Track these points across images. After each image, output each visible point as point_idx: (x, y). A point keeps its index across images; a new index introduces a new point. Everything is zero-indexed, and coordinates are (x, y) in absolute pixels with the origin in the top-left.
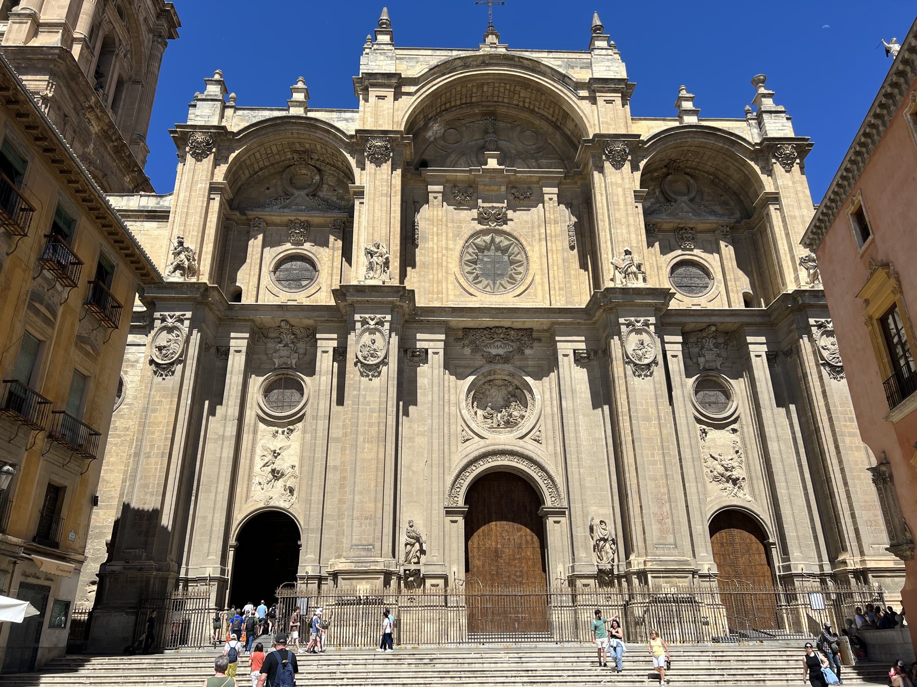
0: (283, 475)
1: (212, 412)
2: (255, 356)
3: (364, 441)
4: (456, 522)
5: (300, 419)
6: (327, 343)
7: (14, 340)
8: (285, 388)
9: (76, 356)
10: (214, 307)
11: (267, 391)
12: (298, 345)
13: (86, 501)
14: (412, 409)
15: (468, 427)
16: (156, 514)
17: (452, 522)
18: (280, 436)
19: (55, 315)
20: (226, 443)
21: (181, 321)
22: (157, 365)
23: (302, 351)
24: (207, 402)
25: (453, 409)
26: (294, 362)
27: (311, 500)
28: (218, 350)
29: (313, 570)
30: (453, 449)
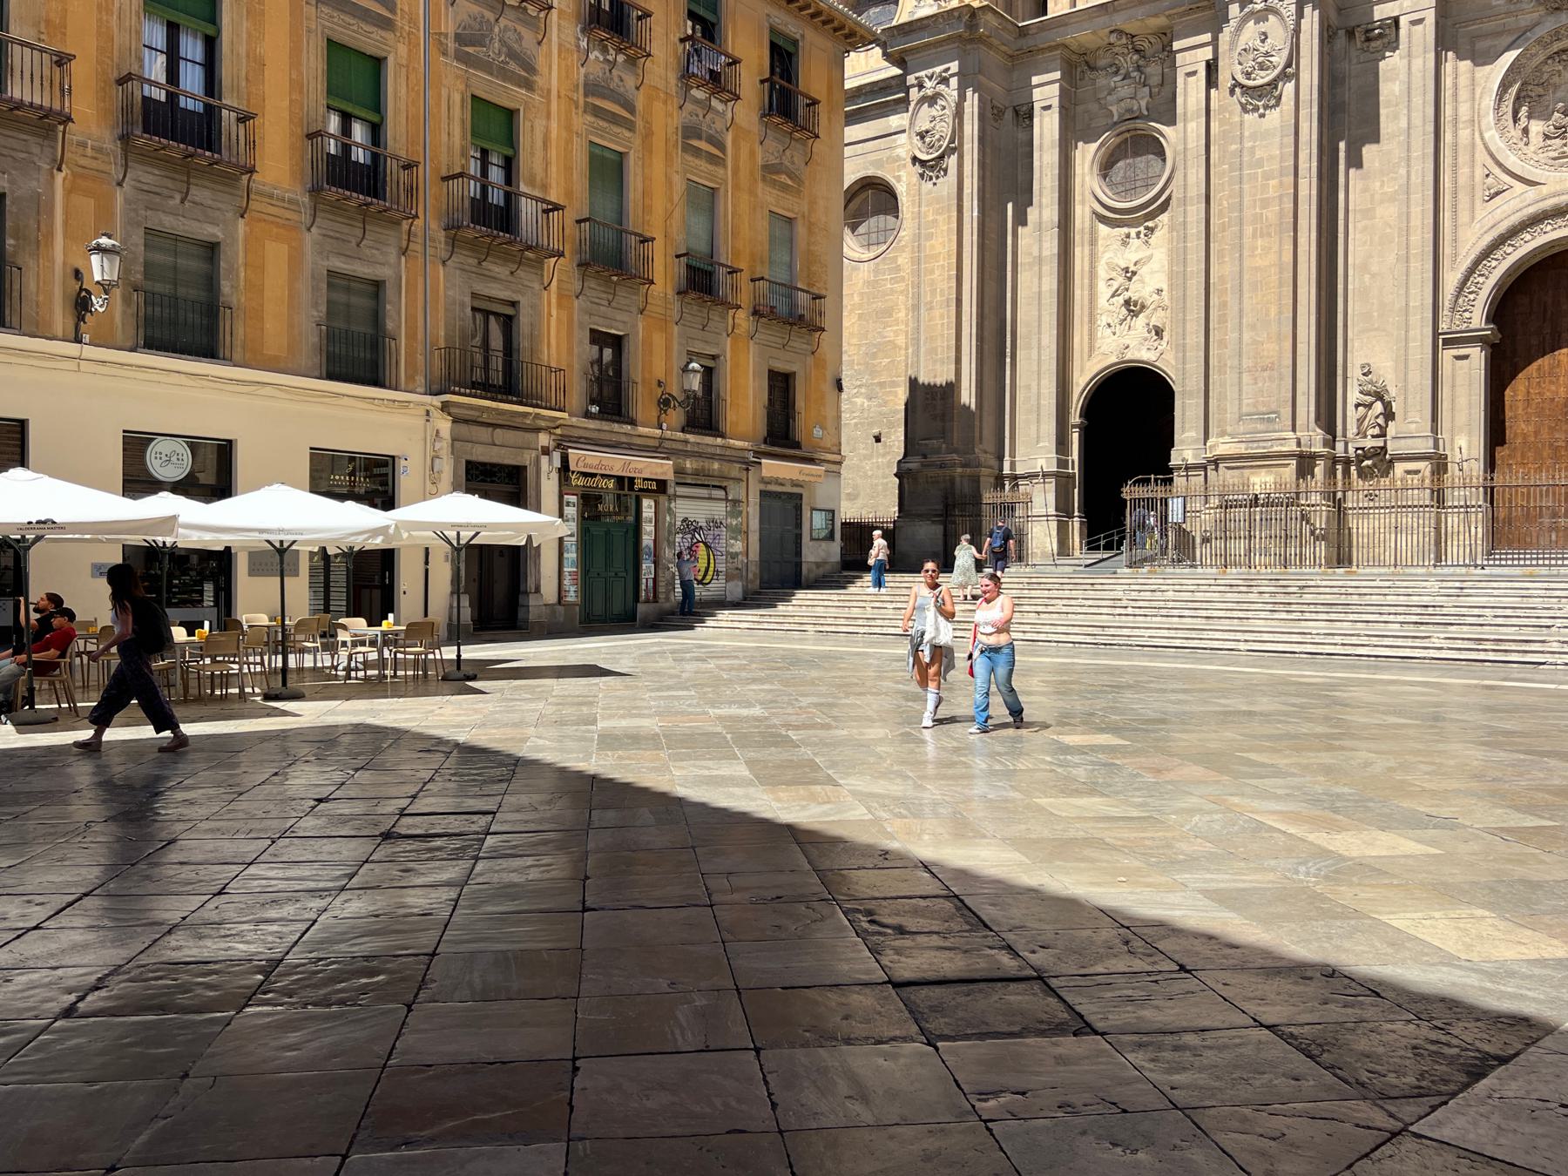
0: (1143, 307)
1: (1021, 220)
2: (1080, 109)
3: (1254, 236)
4: (1466, 357)
5: (1164, 207)
6: (1191, 56)
7: (676, 199)
8: (1136, 154)
9: (770, 198)
10: (995, 42)
11: (1106, 167)
12: (1148, 70)
13: (828, 387)
14: (1368, 151)
15: (1500, 165)
16: (951, 389)
17: (1458, 358)
18: (1134, 242)
19: (721, 146)
20: (1046, 269)
21: (944, 81)
22: (923, 163)
23: (1155, 80)
24: (1010, 206)
25: (1464, 134)
26: (1143, 103)
27: (1184, 346)
28: (1016, 112)
29: (1195, 456)
30: (1464, 217)
